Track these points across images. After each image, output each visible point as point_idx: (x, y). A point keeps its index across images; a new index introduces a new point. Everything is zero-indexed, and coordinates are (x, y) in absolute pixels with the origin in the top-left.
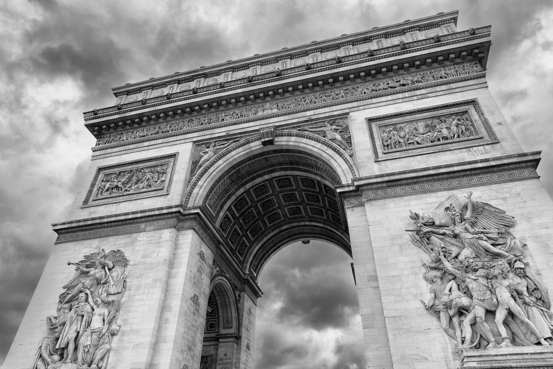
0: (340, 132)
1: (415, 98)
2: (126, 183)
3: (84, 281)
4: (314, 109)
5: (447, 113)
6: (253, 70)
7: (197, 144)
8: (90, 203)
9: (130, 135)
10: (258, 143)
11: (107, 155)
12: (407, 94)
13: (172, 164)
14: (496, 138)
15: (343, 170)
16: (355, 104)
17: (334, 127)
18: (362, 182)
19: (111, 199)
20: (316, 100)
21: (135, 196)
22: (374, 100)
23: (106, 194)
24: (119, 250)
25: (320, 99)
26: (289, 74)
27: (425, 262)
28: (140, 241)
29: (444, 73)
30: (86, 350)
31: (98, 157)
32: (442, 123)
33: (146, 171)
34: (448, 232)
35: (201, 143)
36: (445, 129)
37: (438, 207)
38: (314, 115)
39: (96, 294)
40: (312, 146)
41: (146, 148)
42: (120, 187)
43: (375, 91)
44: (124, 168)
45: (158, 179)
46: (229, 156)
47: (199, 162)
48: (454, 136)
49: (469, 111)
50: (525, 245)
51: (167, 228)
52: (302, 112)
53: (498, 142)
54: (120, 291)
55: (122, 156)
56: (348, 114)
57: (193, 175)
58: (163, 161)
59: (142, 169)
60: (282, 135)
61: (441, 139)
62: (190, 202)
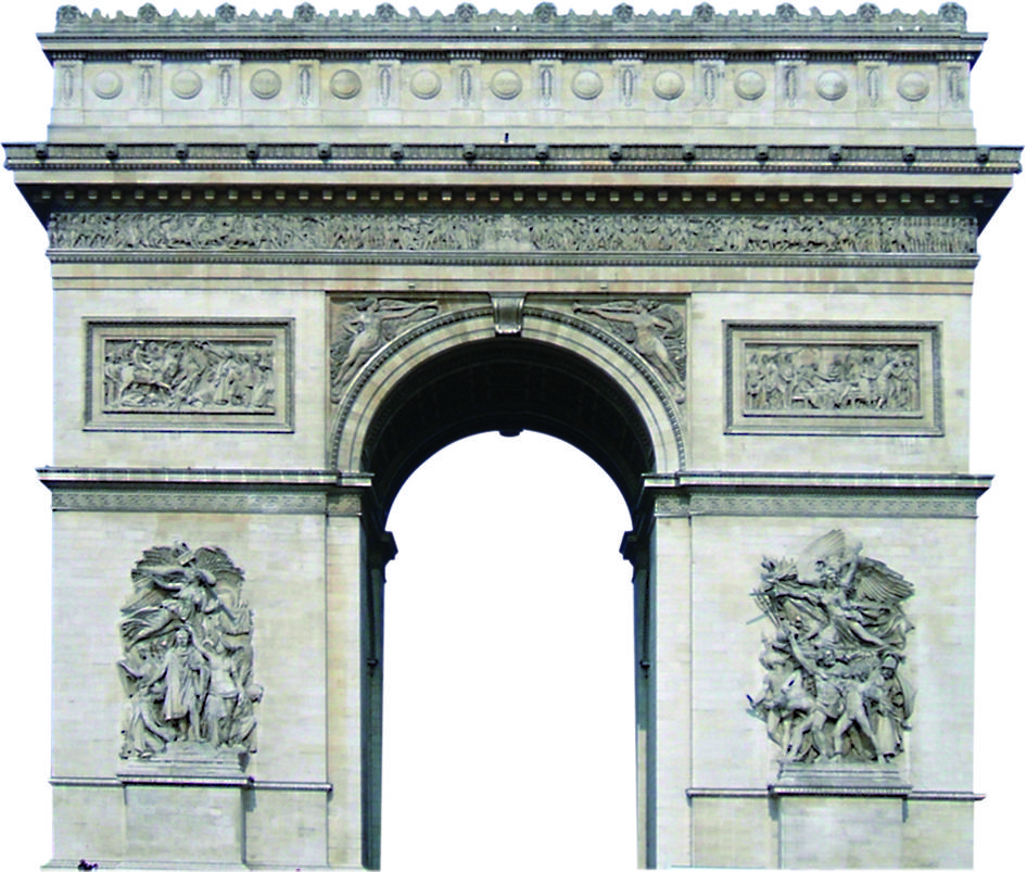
0: (666, 338)
1: (831, 287)
2: (174, 376)
3: (173, 608)
4: (617, 265)
5: (882, 340)
6: (460, 71)
7: (335, 296)
8: (99, 419)
9: (145, 231)
10: (482, 323)
11: (98, 283)
12: (817, 274)
13: (282, 346)
14: (941, 427)
15: (660, 433)
16: (707, 273)
17: (656, 320)
18: (694, 481)
19: (151, 416)
20: (622, 236)
21: (210, 418)
22: (749, 273)
23: (133, 400)
24: (218, 549)
25: (632, 235)
26: (568, 159)
27: (767, 635)
28: (255, 532)
29: (903, 232)
30: (222, 723)
31: (73, 284)
32: (866, 365)
33: (219, 349)
34: (811, 598)
35: (343, 296)
36: (867, 382)
37: (808, 551)
38: (616, 281)
39: (200, 630)
40: (605, 360)
41: (202, 284)
42: (163, 388)
43: (754, 244)
44: (156, 331)
45: (254, 378)
46: (415, 346)
47: (347, 351)
48: (877, 401)
49: (921, 347)
50: (913, 628)
51: (308, 513)
52: (588, 264)
53: (942, 436)
54: (247, 630)
55: (142, 293)
56: (689, 294)
57: (335, 381)
58: (255, 331)
59: (205, 343)
60: (539, 315)
61: (853, 402)
62: (341, 453)
